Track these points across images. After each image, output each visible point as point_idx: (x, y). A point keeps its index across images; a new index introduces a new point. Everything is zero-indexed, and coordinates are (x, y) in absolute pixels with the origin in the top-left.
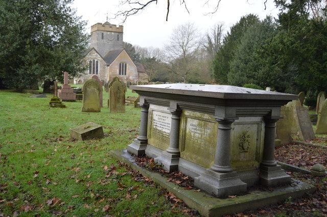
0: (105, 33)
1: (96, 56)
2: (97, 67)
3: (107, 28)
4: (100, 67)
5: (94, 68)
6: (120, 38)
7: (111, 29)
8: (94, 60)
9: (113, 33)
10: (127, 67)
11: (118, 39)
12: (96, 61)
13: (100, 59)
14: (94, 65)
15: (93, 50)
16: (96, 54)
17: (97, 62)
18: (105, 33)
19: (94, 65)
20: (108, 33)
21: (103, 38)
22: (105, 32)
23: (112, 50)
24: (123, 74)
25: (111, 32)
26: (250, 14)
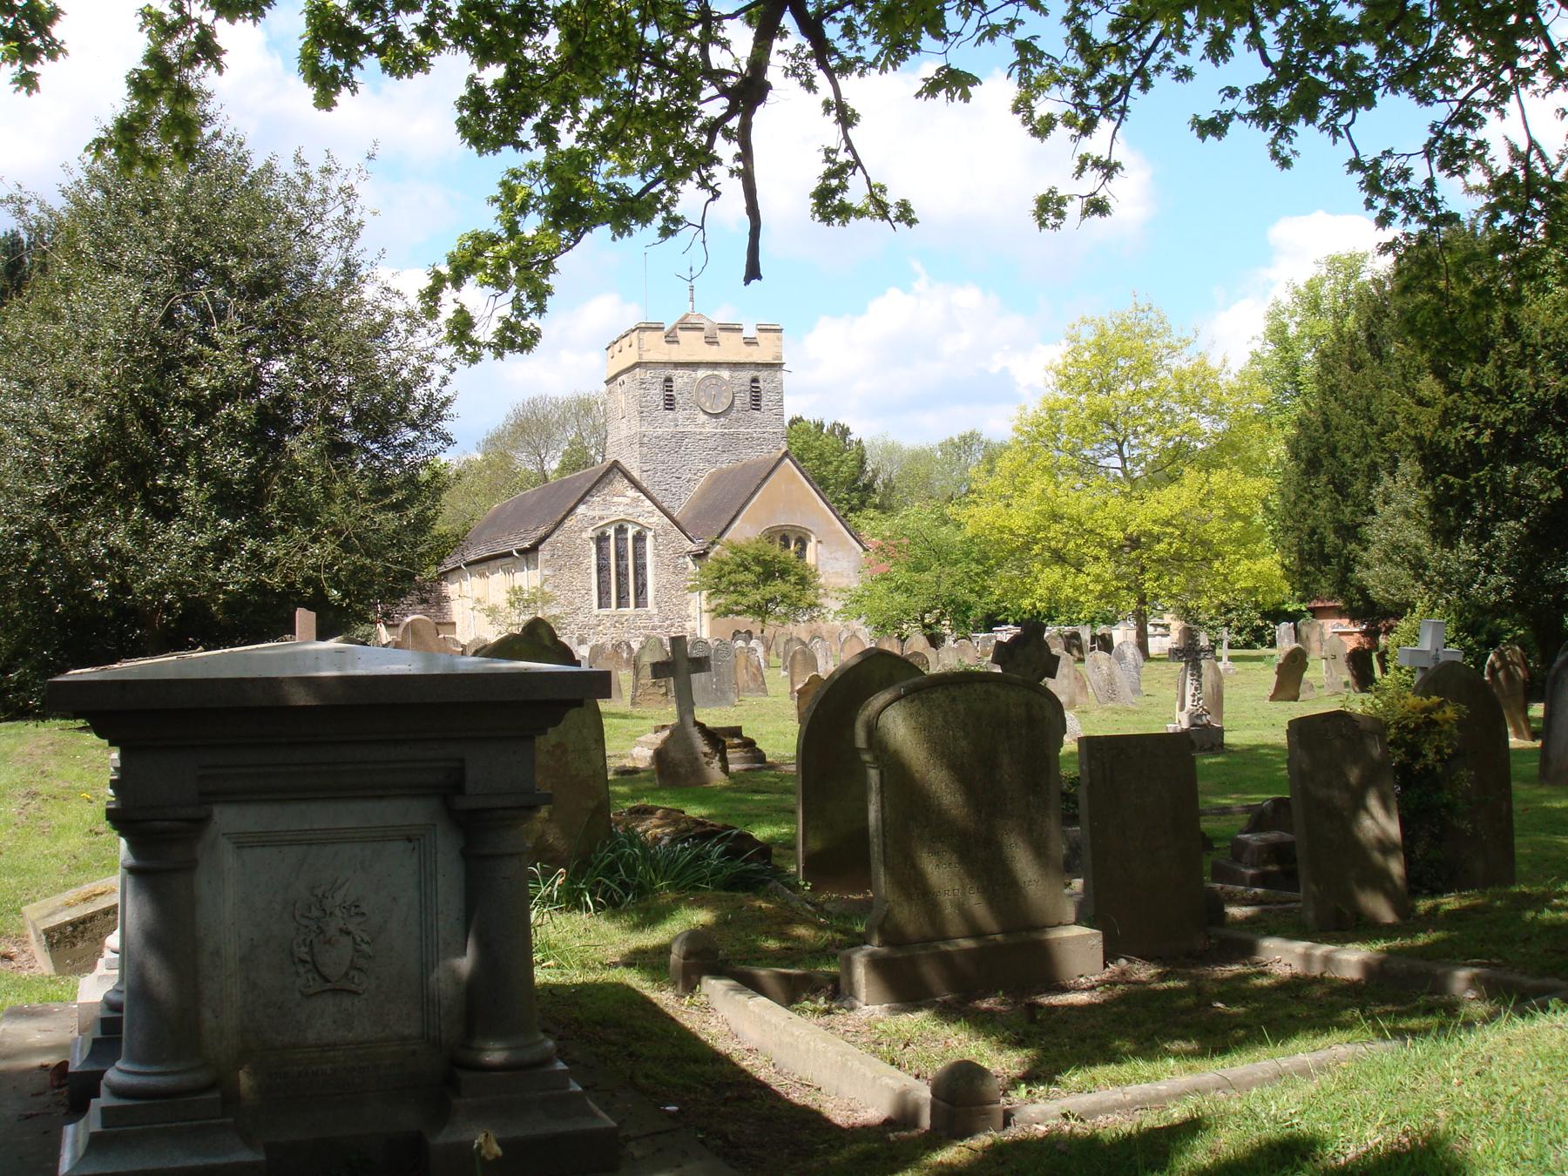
0: (681, 378)
2: (640, 569)
3: (692, 347)
5: (622, 575)
7: (711, 354)
8: (621, 530)
9: (725, 374)
13: (657, 519)
16: (632, 493)
17: (639, 538)
18: (681, 378)
20: (701, 373)
21: (670, 404)
22: (679, 372)
23: (725, 463)
26: (480, 153)
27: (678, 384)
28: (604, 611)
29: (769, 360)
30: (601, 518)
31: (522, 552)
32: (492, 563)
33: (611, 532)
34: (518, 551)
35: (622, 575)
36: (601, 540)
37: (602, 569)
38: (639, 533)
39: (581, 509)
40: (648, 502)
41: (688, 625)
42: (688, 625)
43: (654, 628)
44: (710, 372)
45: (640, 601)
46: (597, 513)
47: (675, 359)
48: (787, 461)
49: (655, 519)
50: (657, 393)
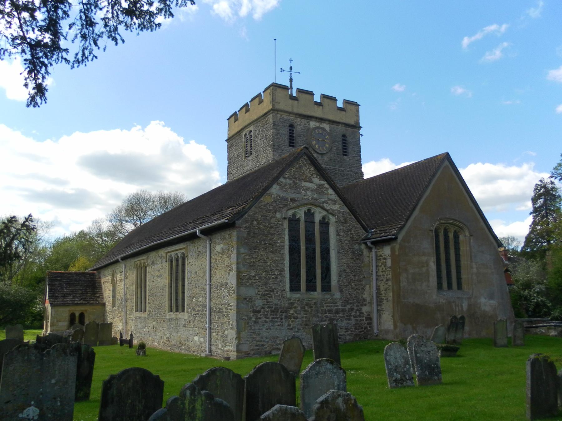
1: (319, 189)
2: (326, 253)
4: (340, 249)
5: (311, 258)
6: (351, 147)
7: (318, 112)
8: (309, 215)
9: (326, 126)
10: (464, 248)
11: (345, 152)
12: (318, 215)
14: (310, 239)
15: (303, 162)
16: (317, 180)
17: (324, 224)
19: (310, 239)
20: (313, 124)
22: (299, 120)
24: (450, 286)
25: (321, 120)
27: (299, 128)
28: (296, 295)
29: (352, 122)
30: (293, 200)
31: (208, 232)
32: (153, 255)
33: (301, 214)
34: (203, 232)
35: (311, 258)
36: (294, 222)
37: (294, 250)
38: (324, 218)
39: (275, 189)
40: (331, 191)
41: (365, 309)
42: (365, 309)
43: (337, 312)
44: (317, 124)
45: (327, 288)
46: (290, 195)
47: (295, 111)
48: (446, 163)
49: (336, 207)
50: (285, 133)
